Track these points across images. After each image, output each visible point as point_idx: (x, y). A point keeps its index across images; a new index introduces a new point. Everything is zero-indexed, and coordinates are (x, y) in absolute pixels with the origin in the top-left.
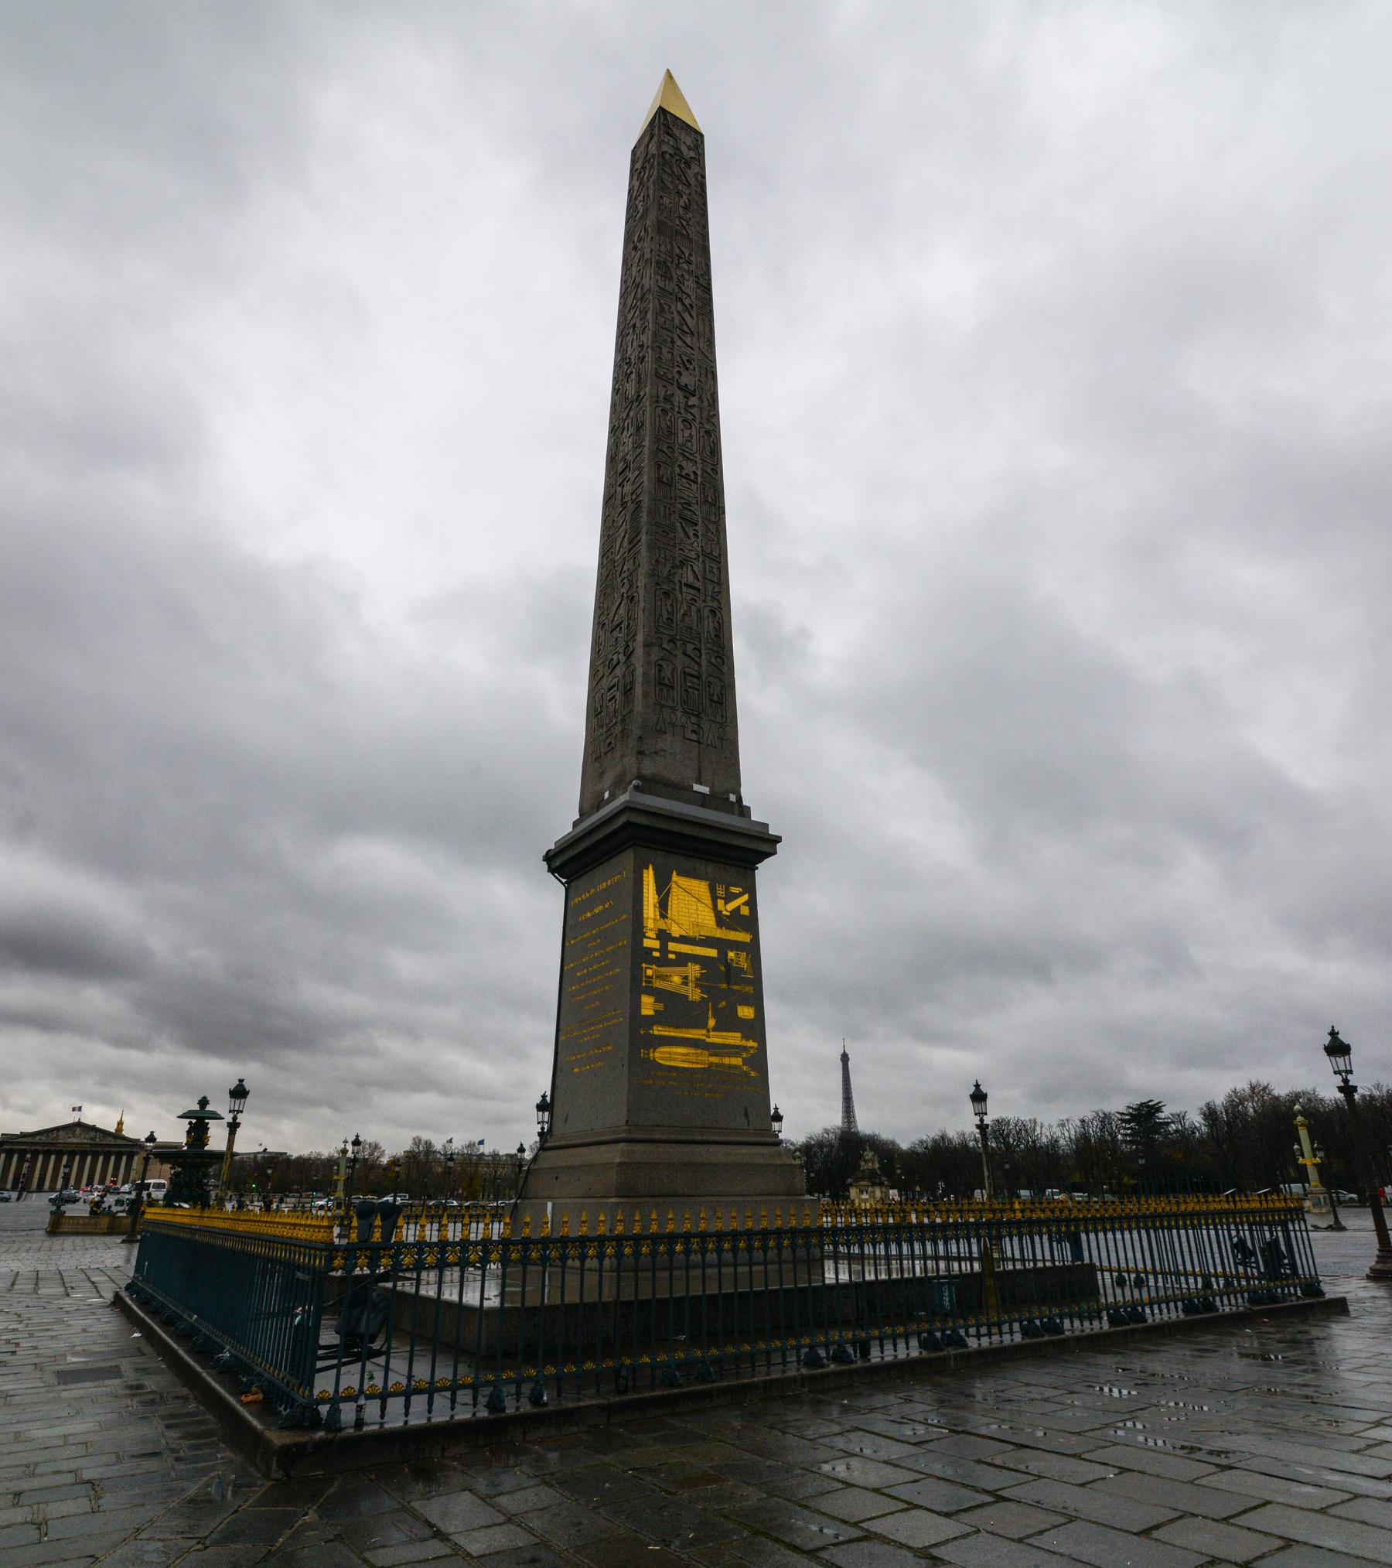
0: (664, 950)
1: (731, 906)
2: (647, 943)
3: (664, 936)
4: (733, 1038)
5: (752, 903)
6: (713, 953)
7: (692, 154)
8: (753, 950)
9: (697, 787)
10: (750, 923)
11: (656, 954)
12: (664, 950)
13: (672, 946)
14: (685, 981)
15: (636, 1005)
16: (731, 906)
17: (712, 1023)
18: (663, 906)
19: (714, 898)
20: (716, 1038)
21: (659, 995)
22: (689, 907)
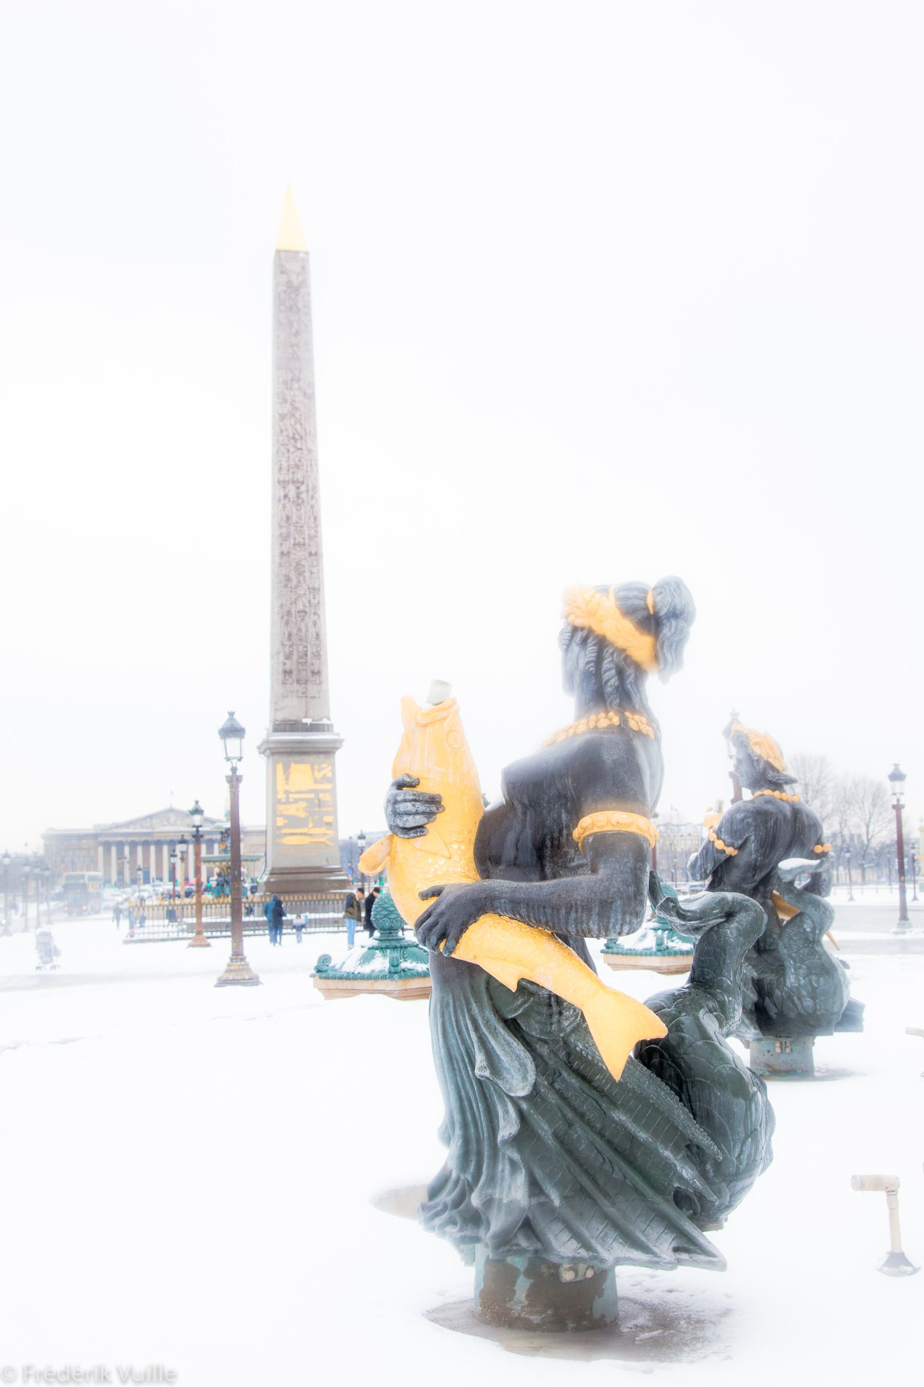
0: (287, 798)
1: (322, 774)
2: (279, 796)
3: (287, 792)
4: (322, 830)
5: (333, 771)
6: (312, 796)
7: (301, 278)
8: (333, 792)
9: (305, 721)
10: (332, 780)
11: (284, 800)
12: (287, 798)
13: (291, 796)
14: (298, 809)
15: (274, 822)
16: (322, 774)
17: (311, 825)
18: (287, 779)
19: (313, 770)
20: (313, 831)
21: (285, 817)
22: (301, 775)
